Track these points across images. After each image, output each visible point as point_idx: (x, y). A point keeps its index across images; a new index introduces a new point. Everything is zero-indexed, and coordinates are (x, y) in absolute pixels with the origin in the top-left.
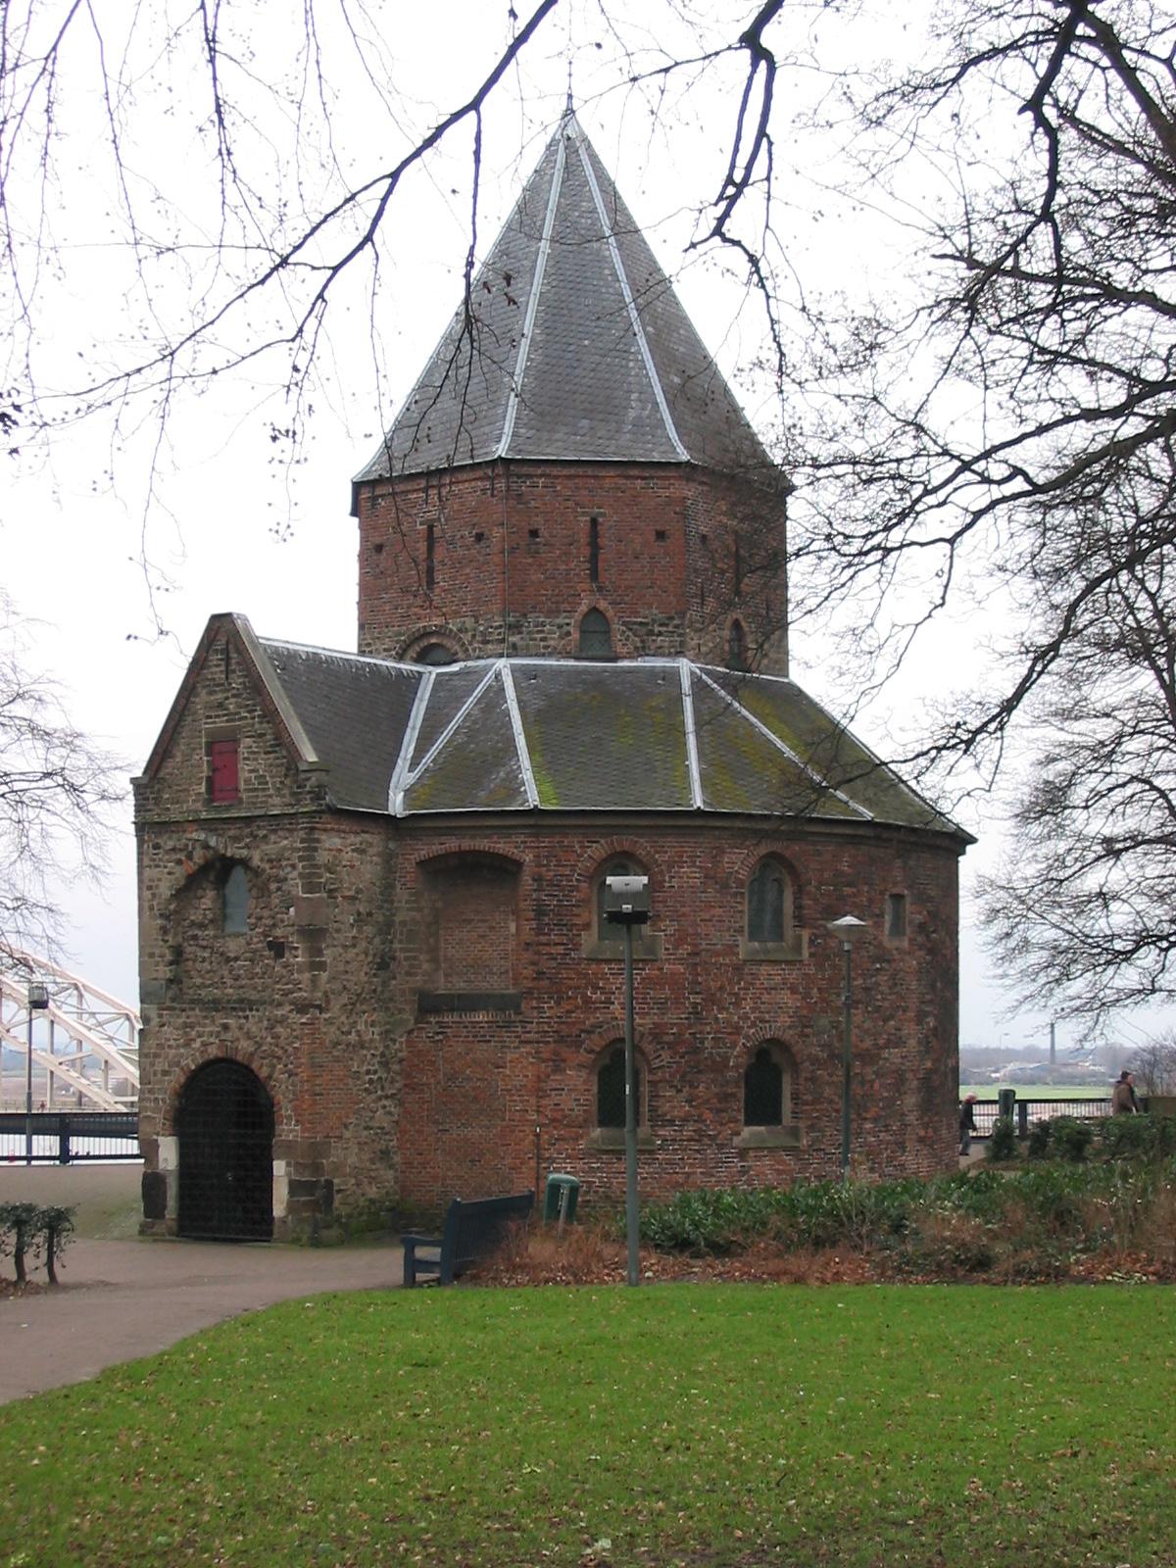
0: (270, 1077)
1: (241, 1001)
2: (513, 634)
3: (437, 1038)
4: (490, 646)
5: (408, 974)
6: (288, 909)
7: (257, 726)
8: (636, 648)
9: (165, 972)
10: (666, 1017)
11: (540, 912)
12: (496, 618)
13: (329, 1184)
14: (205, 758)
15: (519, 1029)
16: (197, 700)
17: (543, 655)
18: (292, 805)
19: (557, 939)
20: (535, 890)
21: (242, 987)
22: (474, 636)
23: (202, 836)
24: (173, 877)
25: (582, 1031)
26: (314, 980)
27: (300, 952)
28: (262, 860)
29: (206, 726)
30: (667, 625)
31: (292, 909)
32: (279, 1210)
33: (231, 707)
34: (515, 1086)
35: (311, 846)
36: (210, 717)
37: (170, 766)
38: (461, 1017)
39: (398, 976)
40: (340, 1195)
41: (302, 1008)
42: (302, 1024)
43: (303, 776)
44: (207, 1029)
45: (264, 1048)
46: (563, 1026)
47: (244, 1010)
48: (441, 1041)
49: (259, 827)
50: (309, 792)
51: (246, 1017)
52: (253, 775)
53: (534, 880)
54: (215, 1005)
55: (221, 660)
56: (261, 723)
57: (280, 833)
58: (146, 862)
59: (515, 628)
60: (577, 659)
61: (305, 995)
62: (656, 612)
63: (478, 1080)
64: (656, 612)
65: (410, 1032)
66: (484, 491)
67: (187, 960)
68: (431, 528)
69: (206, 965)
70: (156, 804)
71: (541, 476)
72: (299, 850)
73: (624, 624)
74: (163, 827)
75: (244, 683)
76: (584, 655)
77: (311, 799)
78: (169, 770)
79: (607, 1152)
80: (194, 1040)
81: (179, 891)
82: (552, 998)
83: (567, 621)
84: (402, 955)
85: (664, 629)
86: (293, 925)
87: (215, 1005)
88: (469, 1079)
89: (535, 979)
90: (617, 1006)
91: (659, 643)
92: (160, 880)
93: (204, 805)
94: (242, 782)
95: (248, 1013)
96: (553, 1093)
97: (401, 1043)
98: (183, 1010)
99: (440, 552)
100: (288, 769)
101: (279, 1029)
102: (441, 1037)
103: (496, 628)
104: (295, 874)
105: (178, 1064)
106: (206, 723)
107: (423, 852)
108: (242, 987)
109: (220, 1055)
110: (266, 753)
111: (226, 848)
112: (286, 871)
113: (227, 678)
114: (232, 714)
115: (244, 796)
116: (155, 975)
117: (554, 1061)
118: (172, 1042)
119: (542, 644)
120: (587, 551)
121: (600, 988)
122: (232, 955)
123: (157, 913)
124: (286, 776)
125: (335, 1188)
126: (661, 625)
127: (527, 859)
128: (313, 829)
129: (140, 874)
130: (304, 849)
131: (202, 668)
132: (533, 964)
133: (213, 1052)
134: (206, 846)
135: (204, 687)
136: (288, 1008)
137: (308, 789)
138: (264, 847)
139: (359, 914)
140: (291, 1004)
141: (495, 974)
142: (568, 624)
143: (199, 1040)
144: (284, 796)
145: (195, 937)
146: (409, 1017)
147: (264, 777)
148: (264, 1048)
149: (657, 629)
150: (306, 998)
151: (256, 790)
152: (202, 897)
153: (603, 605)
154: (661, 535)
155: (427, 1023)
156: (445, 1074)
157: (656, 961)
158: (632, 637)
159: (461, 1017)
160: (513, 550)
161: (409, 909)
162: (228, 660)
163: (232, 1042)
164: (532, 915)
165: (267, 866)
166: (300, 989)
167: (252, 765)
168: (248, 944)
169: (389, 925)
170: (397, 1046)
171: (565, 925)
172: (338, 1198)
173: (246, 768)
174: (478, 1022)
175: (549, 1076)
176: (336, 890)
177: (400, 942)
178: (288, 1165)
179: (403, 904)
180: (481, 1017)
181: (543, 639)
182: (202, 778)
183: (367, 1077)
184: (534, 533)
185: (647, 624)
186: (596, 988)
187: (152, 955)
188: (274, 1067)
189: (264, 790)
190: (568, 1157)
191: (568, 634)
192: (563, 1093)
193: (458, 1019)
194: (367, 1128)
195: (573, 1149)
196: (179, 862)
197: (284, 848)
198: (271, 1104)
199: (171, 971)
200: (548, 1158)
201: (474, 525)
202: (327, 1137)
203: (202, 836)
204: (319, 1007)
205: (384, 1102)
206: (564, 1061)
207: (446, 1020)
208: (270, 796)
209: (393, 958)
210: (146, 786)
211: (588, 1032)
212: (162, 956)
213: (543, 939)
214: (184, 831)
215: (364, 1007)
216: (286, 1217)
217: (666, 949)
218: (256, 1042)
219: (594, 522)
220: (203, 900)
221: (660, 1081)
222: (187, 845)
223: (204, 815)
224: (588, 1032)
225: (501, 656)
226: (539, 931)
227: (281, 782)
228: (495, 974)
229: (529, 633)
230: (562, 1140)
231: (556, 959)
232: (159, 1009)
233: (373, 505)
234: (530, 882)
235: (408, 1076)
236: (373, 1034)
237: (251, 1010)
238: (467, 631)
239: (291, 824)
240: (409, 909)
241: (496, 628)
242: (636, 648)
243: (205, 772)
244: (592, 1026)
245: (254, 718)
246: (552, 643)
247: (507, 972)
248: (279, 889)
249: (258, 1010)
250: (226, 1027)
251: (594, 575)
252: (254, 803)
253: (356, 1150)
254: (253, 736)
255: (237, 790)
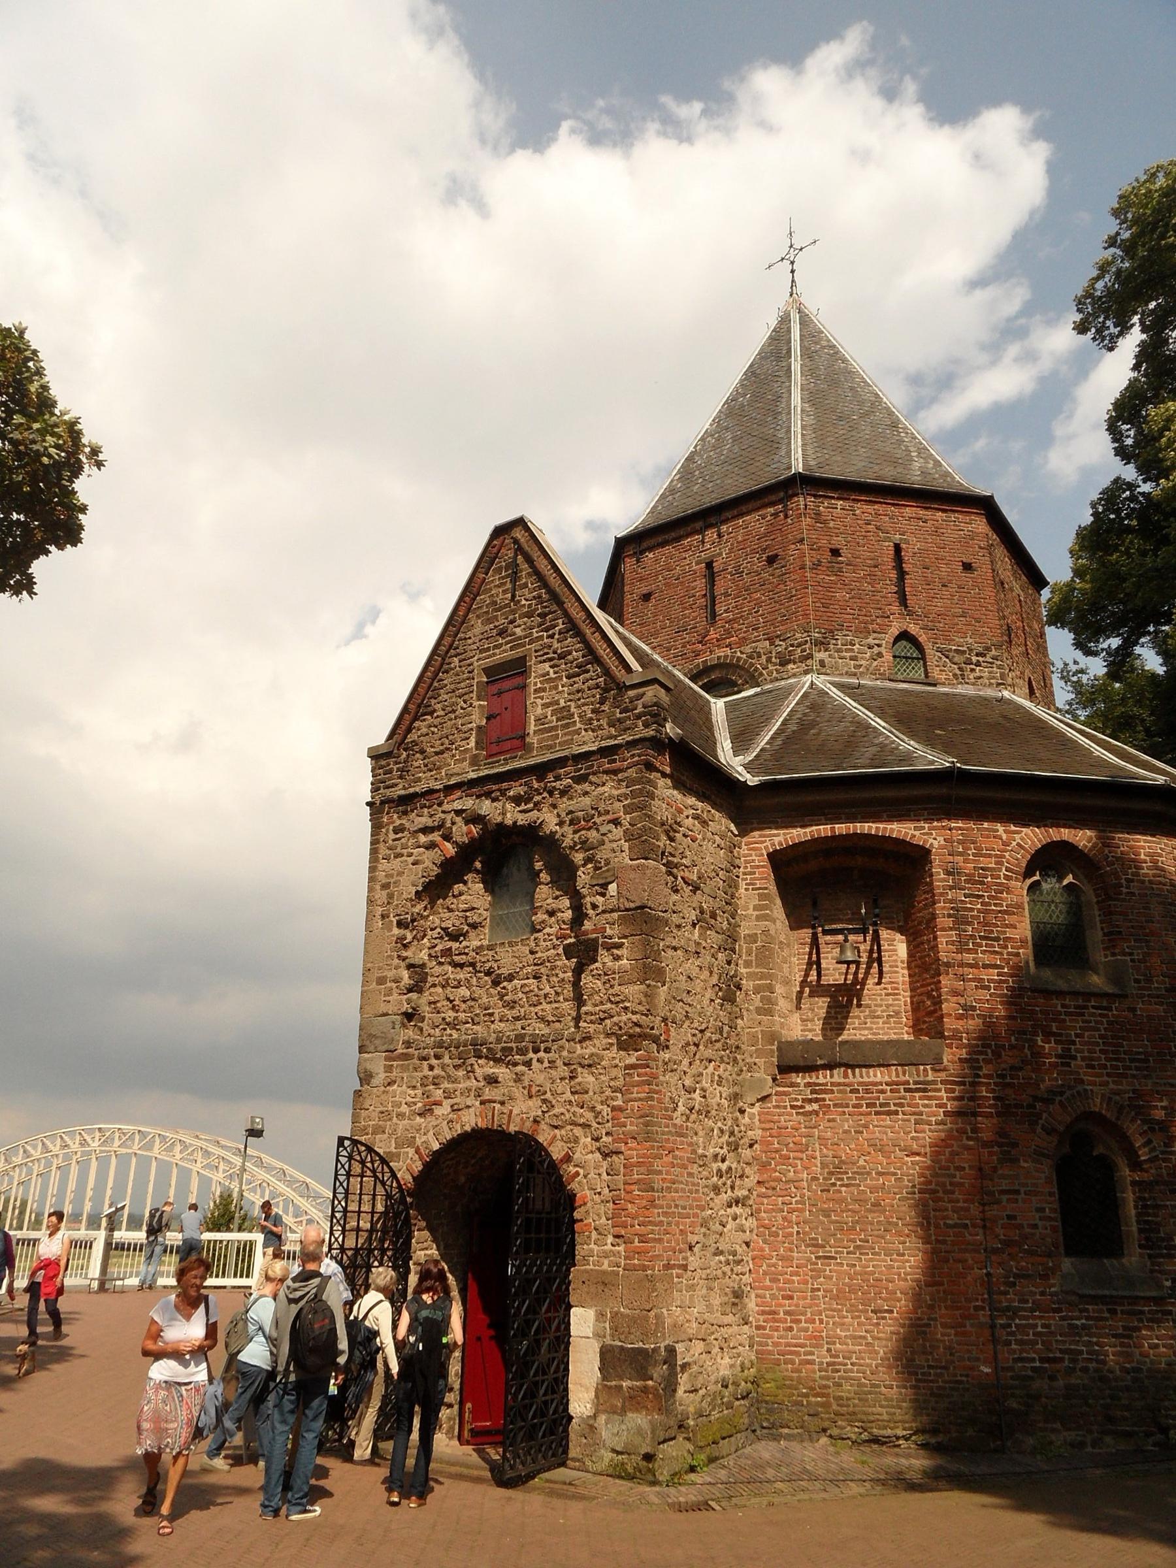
0: (568, 1159)
1: (520, 1038)
2: (820, 651)
3: (808, 1108)
4: (791, 666)
5: (759, 1011)
6: (605, 886)
7: (556, 645)
8: (955, 675)
9: (399, 1002)
10: (1150, 1082)
11: (960, 920)
12: (798, 635)
13: (671, 1351)
14: (476, 703)
15: (943, 1094)
16: (469, 634)
17: (855, 675)
18: (615, 737)
19: (987, 959)
20: (951, 887)
21: (517, 1019)
22: (769, 660)
23: (469, 803)
24: (421, 867)
25: (1036, 1098)
26: (649, 996)
27: (623, 952)
28: (561, 824)
29: (479, 663)
30: (983, 655)
31: (612, 888)
32: (581, 1403)
33: (518, 630)
34: (944, 1184)
35: (641, 802)
36: (488, 649)
37: (422, 726)
38: (846, 1076)
39: (745, 1013)
40: (686, 1375)
41: (628, 1042)
42: (627, 1067)
43: (631, 693)
44: (461, 1086)
45: (556, 1111)
46: (1009, 1091)
47: (522, 1051)
48: (816, 1113)
49: (558, 778)
50: (638, 717)
51: (528, 1064)
52: (549, 711)
53: (948, 873)
54: (479, 1049)
55: (507, 576)
56: (559, 641)
57: (593, 778)
58: (383, 850)
59: (822, 644)
60: (890, 680)
61: (634, 1018)
62: (970, 641)
63: (879, 1174)
64: (970, 641)
65: (763, 1099)
66: (776, 515)
67: (434, 985)
68: (709, 565)
69: (464, 992)
70: (401, 777)
71: (838, 499)
72: (626, 796)
73: (939, 650)
74: (406, 802)
75: (540, 597)
76: (900, 677)
77: (647, 726)
78: (424, 730)
79: (1094, 1299)
80: (438, 1104)
81: (428, 887)
82: (989, 1046)
83: (877, 642)
84: (751, 983)
85: (981, 659)
86: (612, 911)
87: (479, 1049)
88: (863, 1173)
89: (960, 1017)
90: (1079, 1062)
91: (978, 674)
92: (400, 874)
93: (472, 764)
94: (533, 723)
95: (531, 1055)
96: (1004, 1198)
97: (752, 1117)
98: (425, 1059)
99: (720, 586)
100: (606, 690)
101: (586, 1078)
102: (815, 1106)
103: (799, 645)
104: (618, 832)
105: (411, 1142)
106: (479, 659)
107: (776, 840)
108: (517, 1019)
109: (482, 1124)
110: (568, 677)
111: (504, 814)
112: (603, 829)
113: (513, 596)
114: (520, 638)
115: (533, 740)
116: (383, 1008)
117: (1000, 1145)
118: (404, 1109)
119: (852, 662)
120: (894, 575)
121: (1054, 1034)
122: (505, 971)
123: (394, 920)
124: (602, 703)
125: (679, 1363)
126: (977, 655)
127: (936, 843)
128: (650, 767)
129: (372, 869)
130: (633, 794)
131: (478, 594)
132: (955, 993)
133: (471, 1120)
134: (475, 819)
135: (478, 617)
136: (602, 1041)
137: (640, 709)
138: (565, 804)
139: (702, 912)
140: (608, 1035)
141: (878, 1017)
142: (879, 645)
143: (447, 1104)
144: (600, 727)
145: (447, 952)
146: (763, 1074)
147: (567, 708)
148: (556, 1111)
149: (974, 659)
150: (636, 1024)
151: (555, 728)
152: (461, 894)
153: (913, 629)
154: (967, 567)
155: (792, 1085)
156: (824, 1165)
157: (1125, 996)
158: (949, 664)
159: (846, 1076)
160: (817, 565)
161: (758, 918)
162: (515, 577)
163: (502, 1103)
164: (949, 922)
165: (568, 829)
166: (626, 1008)
167: (547, 697)
168: (532, 952)
169: (732, 937)
170: (746, 1120)
171: (997, 939)
172: (684, 1380)
173: (539, 701)
174: (875, 1084)
175: (995, 1169)
176: (676, 866)
177: (748, 964)
178: (600, 1316)
179: (750, 912)
180: (877, 1075)
181: (852, 659)
182: (472, 729)
183: (715, 1166)
184: (835, 552)
185: (964, 652)
186: (1048, 1034)
187: (381, 981)
188: (576, 1140)
189: (567, 726)
190: (1037, 1306)
191: (880, 655)
192: (1019, 1197)
193: (842, 1080)
194: (718, 1252)
195: (1042, 1294)
196: (431, 846)
197: (599, 798)
198: (569, 1202)
199: (409, 1001)
200: (1008, 1309)
201: (765, 549)
202: (668, 1267)
203: (469, 803)
204: (655, 1040)
205: (738, 1210)
206: (1015, 1145)
207: (821, 1080)
208: (578, 732)
209: (739, 987)
210: (388, 755)
211: (1046, 1101)
212: (397, 981)
213: (969, 958)
214: (440, 805)
215: (709, 1053)
216: (595, 1416)
217: (1137, 981)
218: (544, 1101)
219: (898, 549)
220: (463, 898)
221: (1157, 1183)
222: (443, 821)
223: (473, 775)
224: (1046, 1101)
225: (806, 672)
226: (961, 947)
227: (593, 711)
228: (878, 1017)
229: (839, 651)
230: (1027, 1277)
231: (988, 988)
232: (387, 1059)
233: (638, 561)
234: (942, 876)
235: (764, 1166)
236: (718, 1096)
237: (536, 1051)
238: (759, 656)
239: (614, 761)
240: (758, 918)
241: (799, 645)
242: (955, 675)
243: (477, 719)
244: (1050, 1091)
245: (552, 636)
246: (863, 662)
247: (897, 1013)
248: (588, 860)
249: (547, 1050)
250: (492, 1081)
251: (903, 600)
252: (550, 747)
253: (704, 1291)
254: (551, 660)
255: (523, 737)
